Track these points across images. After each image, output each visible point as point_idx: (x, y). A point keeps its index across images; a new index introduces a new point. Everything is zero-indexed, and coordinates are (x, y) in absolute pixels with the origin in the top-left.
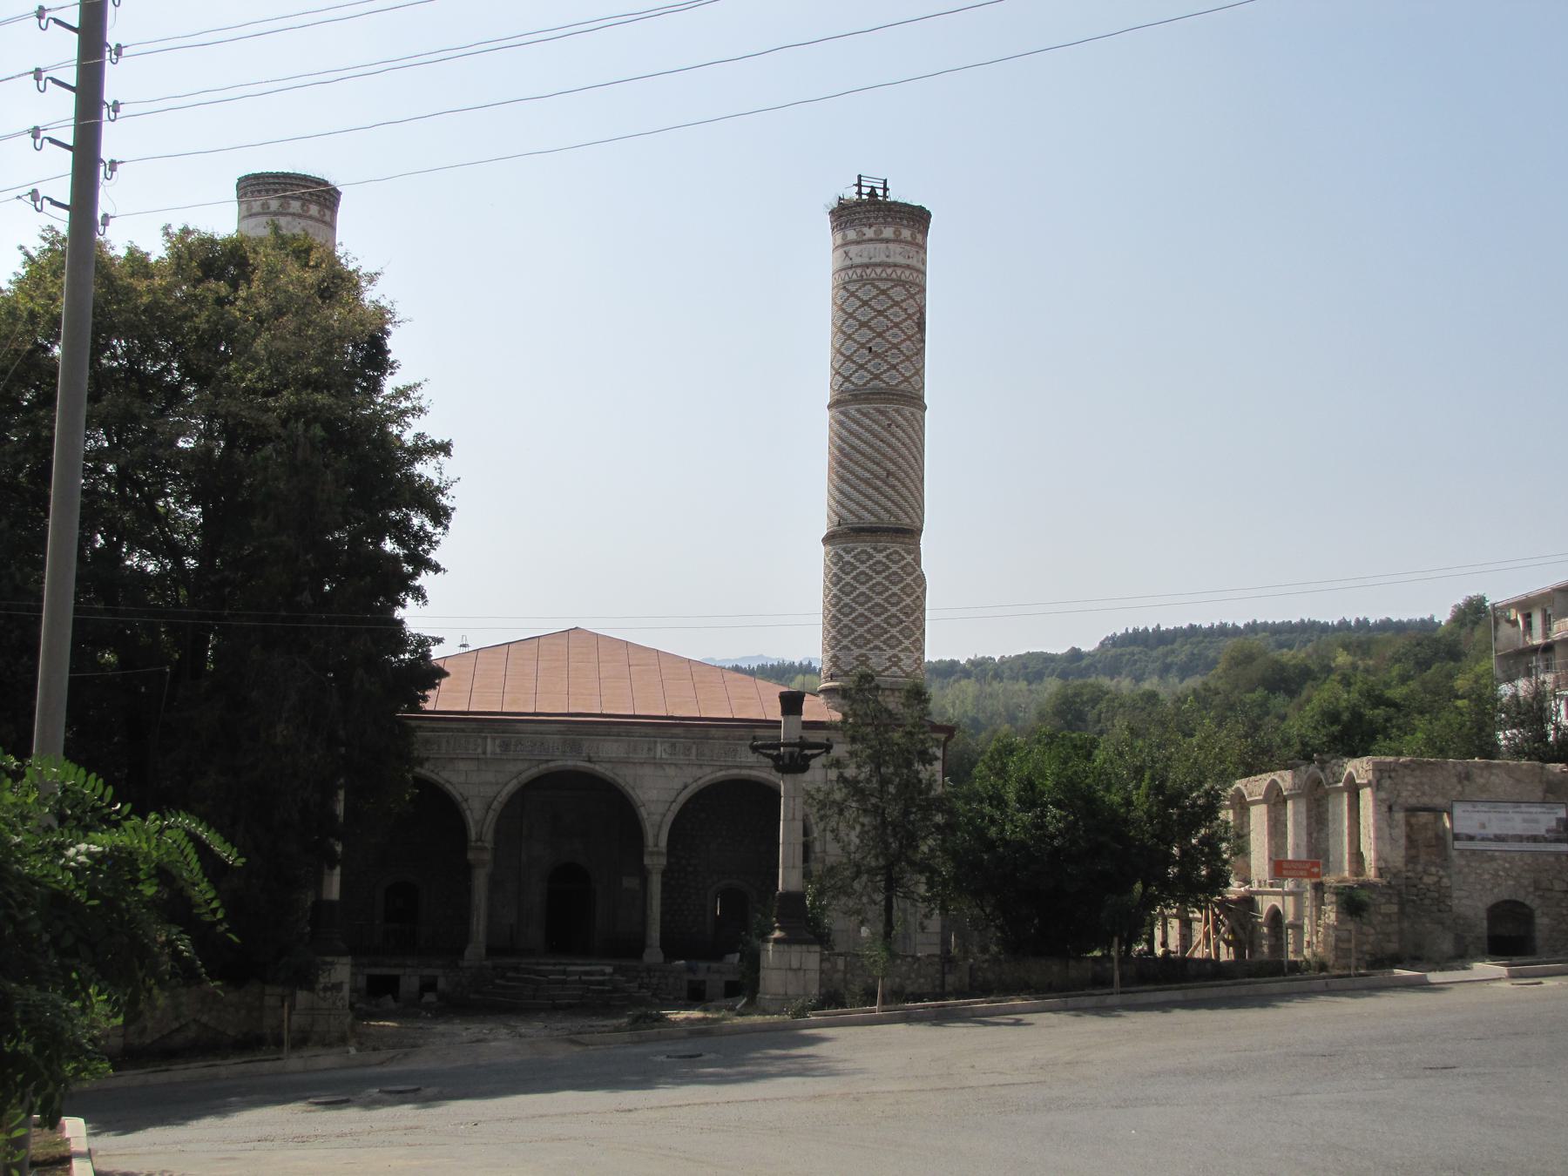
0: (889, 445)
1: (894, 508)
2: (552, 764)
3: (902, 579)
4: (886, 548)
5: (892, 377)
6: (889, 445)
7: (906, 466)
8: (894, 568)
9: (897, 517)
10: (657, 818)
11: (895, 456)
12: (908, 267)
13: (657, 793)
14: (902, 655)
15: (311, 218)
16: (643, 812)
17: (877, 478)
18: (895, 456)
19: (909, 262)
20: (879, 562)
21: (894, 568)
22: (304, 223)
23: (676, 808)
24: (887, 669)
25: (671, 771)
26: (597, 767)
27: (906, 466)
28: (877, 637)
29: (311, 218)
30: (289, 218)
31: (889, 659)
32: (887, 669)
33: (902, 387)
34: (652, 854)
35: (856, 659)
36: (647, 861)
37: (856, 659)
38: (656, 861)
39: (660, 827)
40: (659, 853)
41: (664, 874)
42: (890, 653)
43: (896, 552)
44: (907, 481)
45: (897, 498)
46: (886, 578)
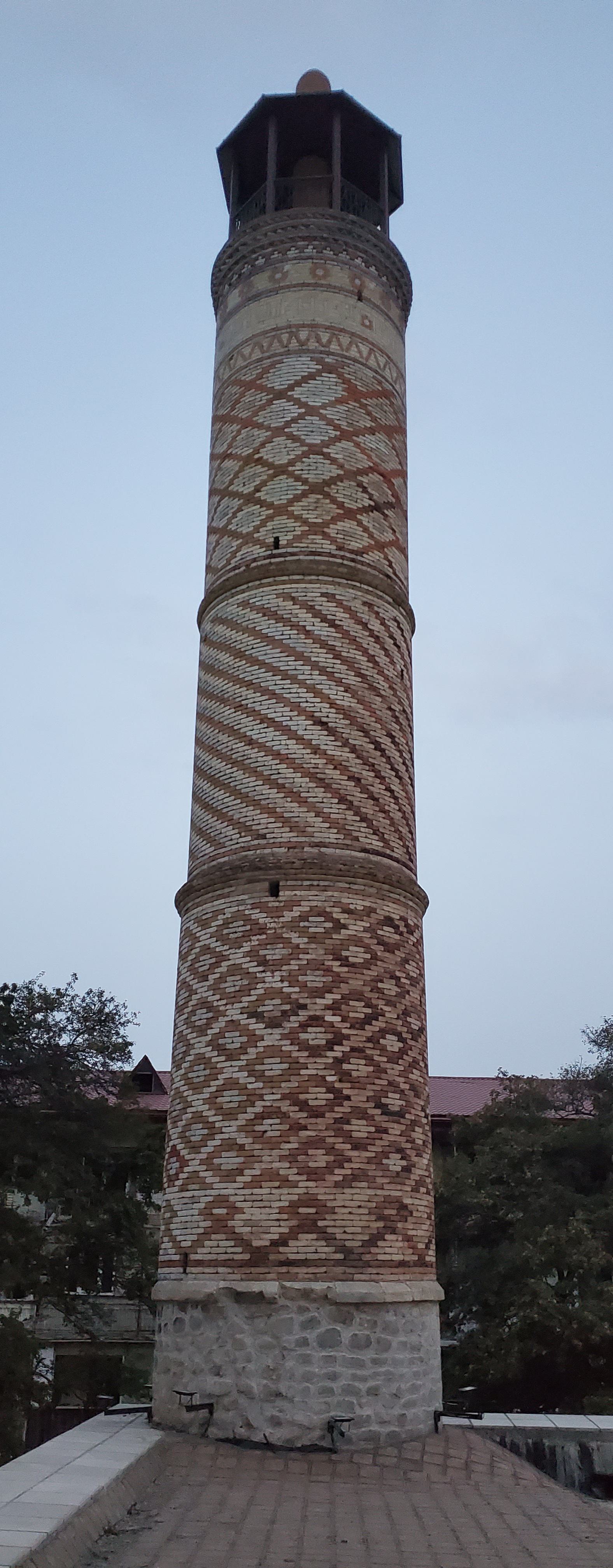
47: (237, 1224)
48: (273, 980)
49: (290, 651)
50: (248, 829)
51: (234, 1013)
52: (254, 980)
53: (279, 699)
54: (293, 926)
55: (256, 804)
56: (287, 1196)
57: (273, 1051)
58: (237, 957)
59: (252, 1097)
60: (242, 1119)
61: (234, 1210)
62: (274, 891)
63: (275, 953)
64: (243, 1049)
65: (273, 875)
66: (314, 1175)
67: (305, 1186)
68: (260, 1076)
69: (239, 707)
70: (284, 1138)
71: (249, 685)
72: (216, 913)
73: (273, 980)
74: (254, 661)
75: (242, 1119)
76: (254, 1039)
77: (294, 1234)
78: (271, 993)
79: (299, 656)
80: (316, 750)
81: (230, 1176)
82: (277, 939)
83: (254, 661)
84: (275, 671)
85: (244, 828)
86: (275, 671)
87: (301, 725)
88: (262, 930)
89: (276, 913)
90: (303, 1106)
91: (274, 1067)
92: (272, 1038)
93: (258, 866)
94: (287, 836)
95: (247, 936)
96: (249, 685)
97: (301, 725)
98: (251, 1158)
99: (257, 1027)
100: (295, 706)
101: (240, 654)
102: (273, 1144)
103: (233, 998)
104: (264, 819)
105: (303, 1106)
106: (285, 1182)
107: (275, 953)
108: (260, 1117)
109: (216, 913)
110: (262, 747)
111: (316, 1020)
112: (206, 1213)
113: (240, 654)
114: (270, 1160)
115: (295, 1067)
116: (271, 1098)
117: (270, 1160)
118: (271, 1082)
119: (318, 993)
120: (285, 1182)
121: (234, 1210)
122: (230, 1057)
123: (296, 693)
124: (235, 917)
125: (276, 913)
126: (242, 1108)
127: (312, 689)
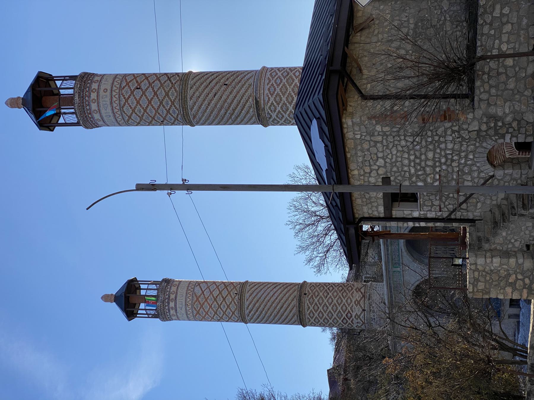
1: (245, 109)
2: (404, 251)
3: (284, 103)
5: (174, 112)
6: (211, 113)
7: (221, 102)
8: (279, 108)
9: (250, 107)
12: (111, 103)
15: (175, 305)
18: (216, 110)
19: (109, 103)
20: (277, 116)
21: (279, 108)
22: (178, 309)
27: (221, 102)
29: (175, 305)
30: (178, 314)
33: (178, 106)
43: (270, 108)
44: (229, 101)
45: (239, 108)
47: (358, 299)
48: (321, 294)
49: (259, 292)
50: (293, 299)
51: (325, 301)
52: (321, 297)
53: (269, 293)
54: (312, 291)
55: (289, 297)
56: (355, 292)
57: (333, 294)
58: (316, 300)
59: (340, 297)
60: (343, 299)
61: (357, 300)
62: (305, 294)
63: (317, 294)
64: (332, 299)
65: (303, 294)
66: (352, 289)
67: (354, 290)
68: (336, 296)
69: (269, 301)
70: (346, 292)
71: (265, 299)
72: (308, 305)
73: (321, 294)
74: (260, 298)
75: (343, 299)
76: (330, 297)
77: (360, 291)
78: (323, 294)
79: (261, 290)
80: (280, 288)
81: (351, 301)
82: (314, 293)
83: (260, 298)
84: (263, 294)
85: (293, 300)
86: (263, 294)
87: (275, 290)
88: (312, 296)
89: (309, 293)
90: (342, 290)
91: (335, 294)
92: (330, 294)
93: (300, 296)
94: (296, 292)
95: (313, 298)
96: (265, 299)
97: (275, 290)
98: (349, 297)
99: (329, 296)
100: (271, 291)
101: (258, 301)
102: (347, 294)
103: (323, 301)
104: (292, 296)
105: (342, 290)
106: (353, 292)
107: (317, 294)
108: (343, 296)
109: (308, 305)
110: (278, 296)
111: (328, 288)
112: (357, 305)
113: (258, 301)
114: (349, 295)
115: (336, 291)
116: (340, 294)
117: (349, 295)
118: (338, 294)
119: (324, 288)
120: (353, 292)
121: (357, 300)
122: (333, 301)
123: (268, 291)
124: (309, 300)
125: (309, 293)
126: (341, 299)
127: (268, 288)
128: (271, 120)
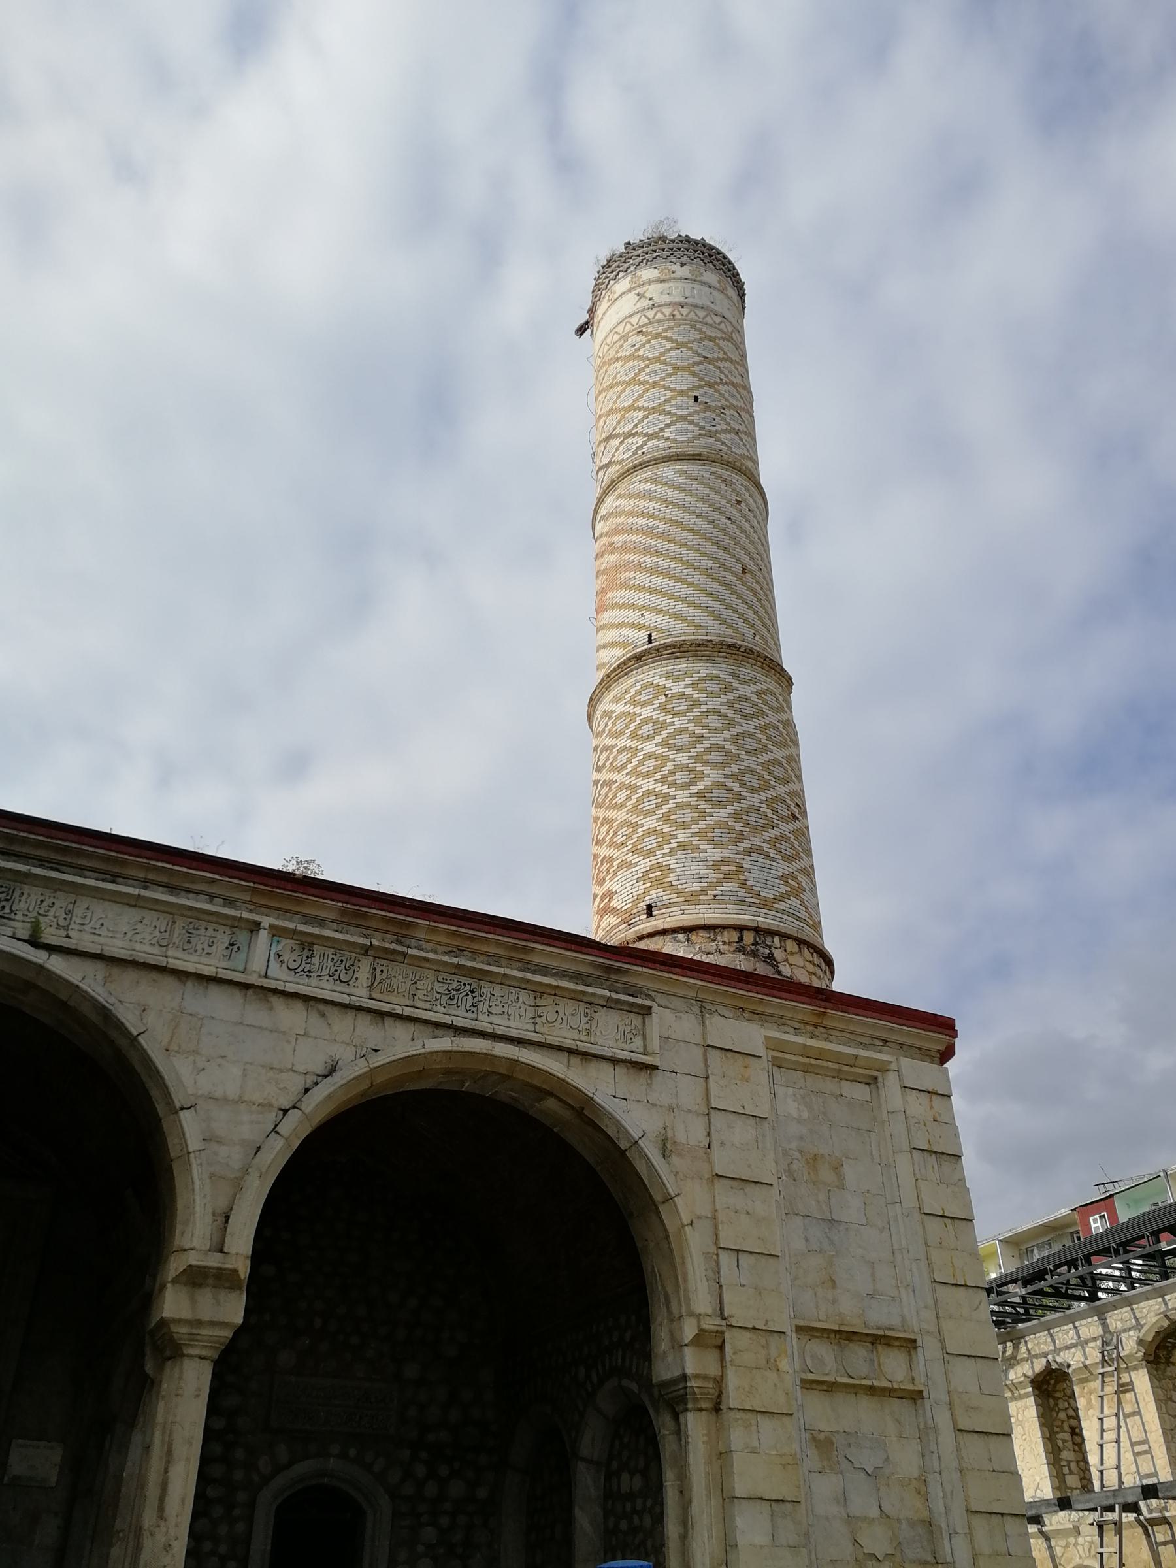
0: (743, 531)
4: (754, 681)
10: (232, 1156)
11: (752, 549)
13: (241, 1092)
14: (802, 878)
16: (191, 1129)
17: (727, 569)
23: (295, 1128)
24: (781, 898)
25: (292, 1017)
26: (57, 964)
28: (756, 829)
31: (784, 878)
32: (781, 898)
34: (196, 1278)
35: (716, 868)
36: (173, 1304)
37: (716, 868)
38: (200, 1307)
39: (238, 1186)
40: (222, 1279)
41: (229, 1366)
42: (782, 867)
46: (763, 729)
128: (729, 678)
